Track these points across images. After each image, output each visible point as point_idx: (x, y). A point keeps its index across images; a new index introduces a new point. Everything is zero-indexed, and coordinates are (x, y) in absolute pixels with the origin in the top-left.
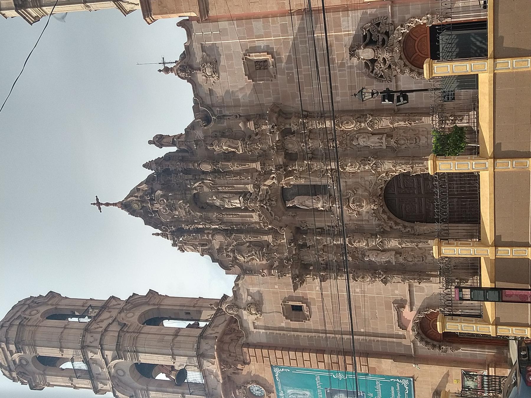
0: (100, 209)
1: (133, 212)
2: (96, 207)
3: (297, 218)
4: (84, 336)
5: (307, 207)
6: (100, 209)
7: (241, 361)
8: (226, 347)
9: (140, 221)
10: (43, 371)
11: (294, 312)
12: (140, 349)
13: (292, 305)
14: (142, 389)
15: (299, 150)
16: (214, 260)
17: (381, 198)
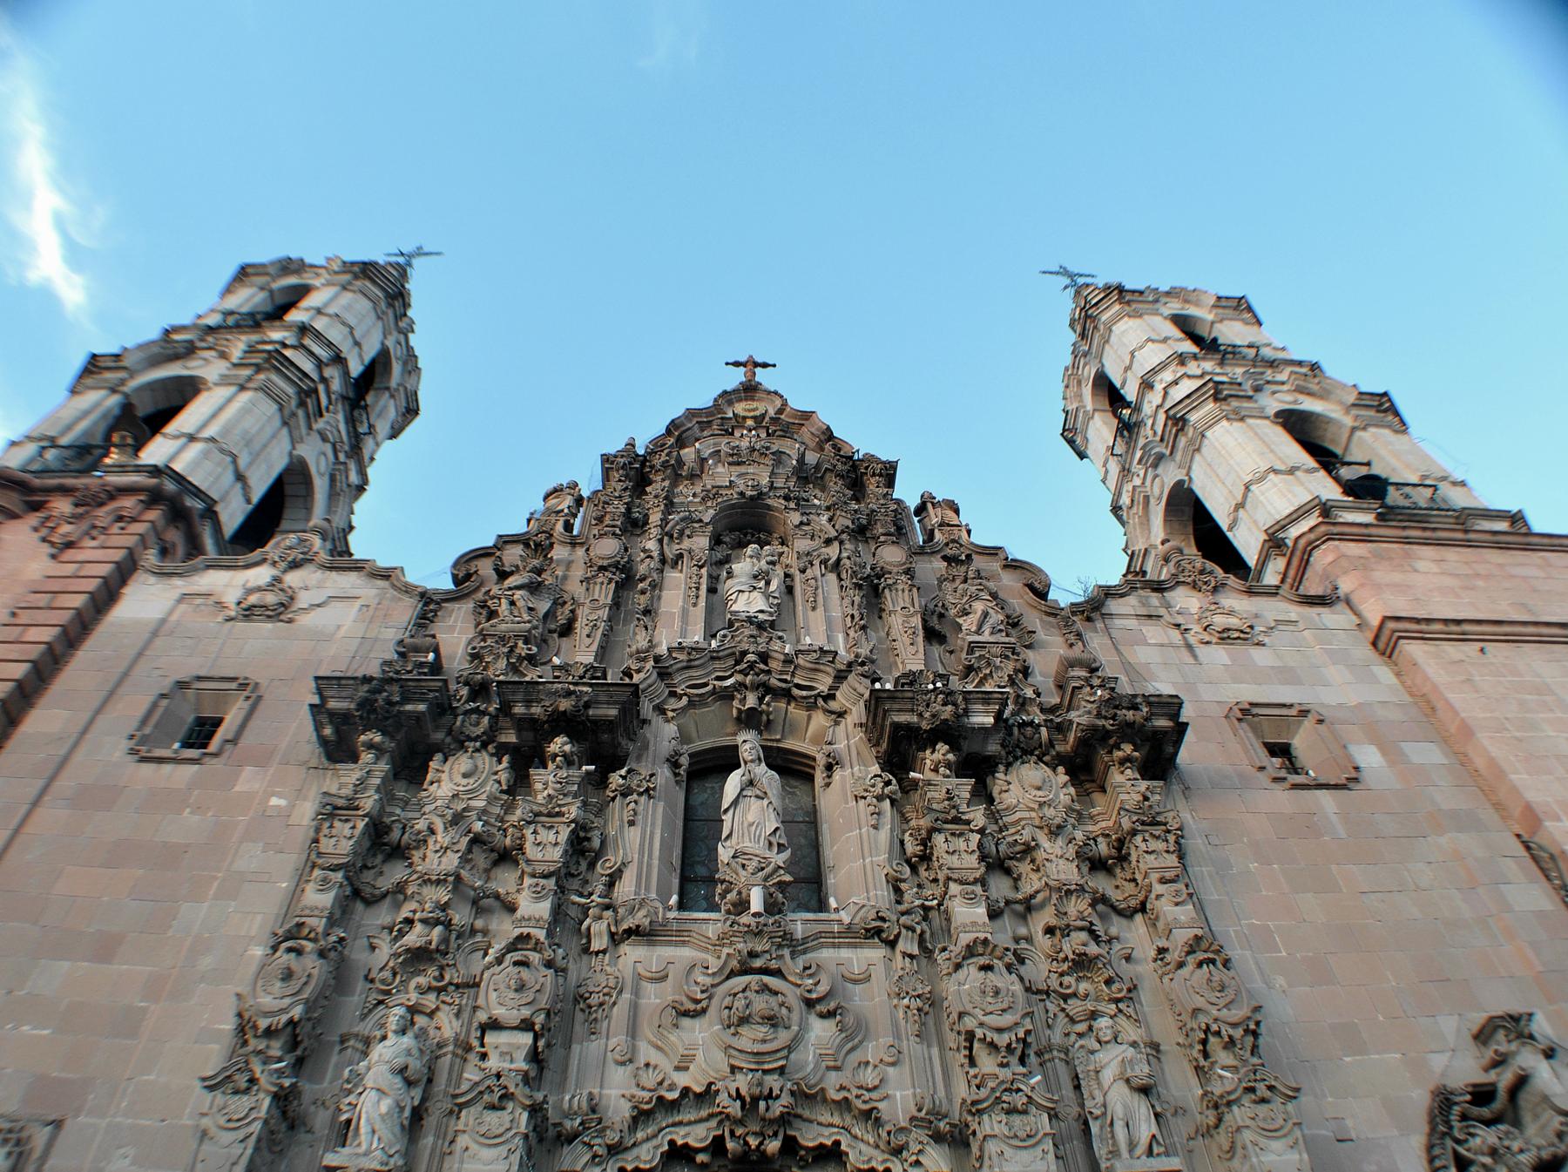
0: (737, 364)
1: (727, 397)
2: (743, 359)
3: (664, 774)
4: (330, 344)
5: (735, 803)
6: (737, 364)
7: (80, 539)
8: (154, 515)
9: (704, 400)
10: (271, 292)
11: (191, 718)
12: (246, 396)
13: (218, 722)
14: (123, 382)
15: (1011, 809)
16: (505, 541)
17: (773, 1146)
